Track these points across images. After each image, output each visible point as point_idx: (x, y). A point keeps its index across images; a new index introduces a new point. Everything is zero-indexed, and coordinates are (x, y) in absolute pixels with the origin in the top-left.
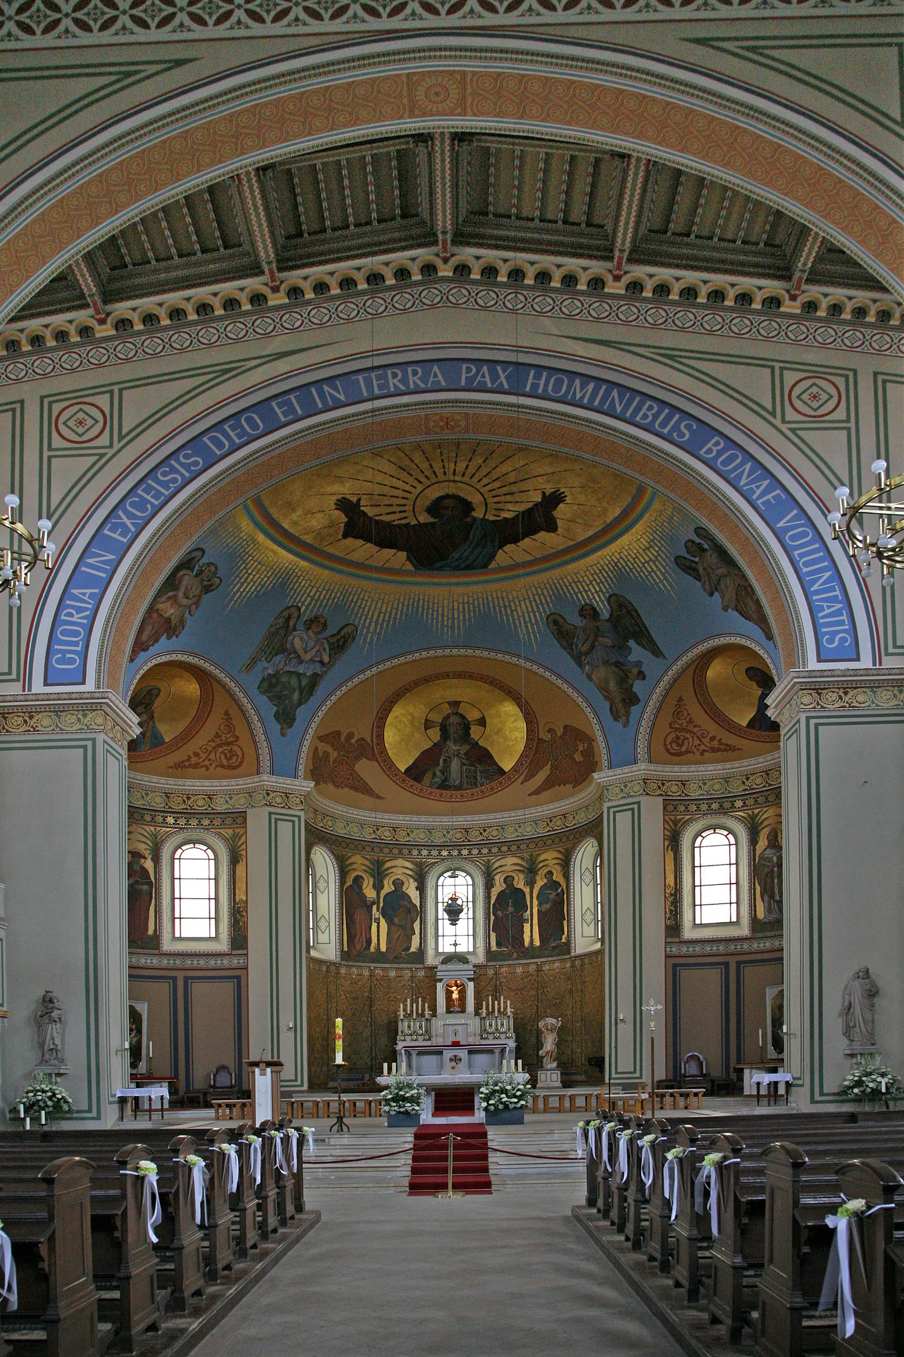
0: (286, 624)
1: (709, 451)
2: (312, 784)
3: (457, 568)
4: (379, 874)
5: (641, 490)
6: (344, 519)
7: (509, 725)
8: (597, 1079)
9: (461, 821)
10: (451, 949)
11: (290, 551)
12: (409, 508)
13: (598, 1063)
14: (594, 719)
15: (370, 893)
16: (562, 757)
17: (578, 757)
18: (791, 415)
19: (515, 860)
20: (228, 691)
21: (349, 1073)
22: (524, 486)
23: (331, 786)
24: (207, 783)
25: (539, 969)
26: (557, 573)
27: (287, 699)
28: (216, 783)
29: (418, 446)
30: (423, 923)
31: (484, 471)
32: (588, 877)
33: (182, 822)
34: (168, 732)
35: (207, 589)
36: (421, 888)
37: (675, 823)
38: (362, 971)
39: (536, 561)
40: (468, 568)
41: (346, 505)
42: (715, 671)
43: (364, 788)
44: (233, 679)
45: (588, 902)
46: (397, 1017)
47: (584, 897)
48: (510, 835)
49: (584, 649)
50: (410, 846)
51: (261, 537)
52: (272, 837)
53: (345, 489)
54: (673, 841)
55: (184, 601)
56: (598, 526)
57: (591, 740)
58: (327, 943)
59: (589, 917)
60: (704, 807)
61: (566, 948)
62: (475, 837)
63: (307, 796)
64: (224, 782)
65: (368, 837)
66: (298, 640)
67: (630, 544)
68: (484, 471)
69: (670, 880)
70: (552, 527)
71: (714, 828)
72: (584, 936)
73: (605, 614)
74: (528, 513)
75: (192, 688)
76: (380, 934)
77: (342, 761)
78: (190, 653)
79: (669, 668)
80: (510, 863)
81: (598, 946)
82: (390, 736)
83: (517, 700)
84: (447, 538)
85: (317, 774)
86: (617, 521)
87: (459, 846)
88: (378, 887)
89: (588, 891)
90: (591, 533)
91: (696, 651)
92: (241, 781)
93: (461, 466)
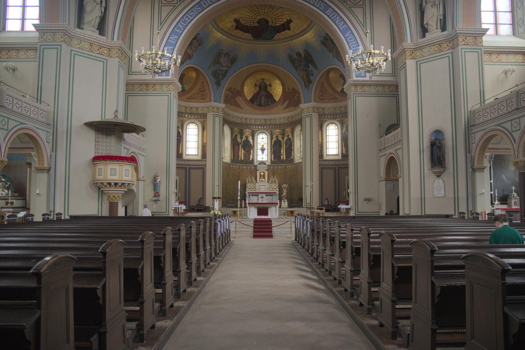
0: (219, 56)
1: (328, 12)
2: (225, 105)
3: (264, 39)
4: (242, 134)
5: (312, 21)
6: (236, 24)
7: (278, 87)
8: (300, 206)
9: (265, 117)
10: (261, 160)
11: (221, 33)
12: (252, 22)
13: (301, 200)
14: (300, 88)
15: (239, 140)
16: (292, 98)
17: (296, 98)
18: (349, 3)
19: (279, 131)
20: (203, 75)
21: (232, 199)
22: (283, 17)
23: (229, 105)
24: (197, 104)
25: (285, 168)
26: (290, 42)
27: (219, 77)
28: (199, 104)
29: (255, 5)
30: (253, 150)
31: (272, 12)
32: (298, 137)
33: (190, 116)
34: (187, 88)
35: (200, 45)
36: (253, 139)
37: (322, 121)
38: (237, 166)
39: (285, 39)
40: (267, 39)
41: (236, 21)
42: (332, 75)
43: (238, 106)
44: (205, 72)
45: (299, 146)
46: (246, 182)
47: (298, 144)
48: (278, 123)
49: (298, 65)
50: (250, 125)
51: (214, 30)
52: (214, 121)
53: (236, 16)
54: (321, 127)
55: (193, 49)
56: (301, 29)
57: (299, 94)
58: (227, 157)
59: (299, 150)
60: (329, 117)
61: (292, 161)
62: (268, 123)
63: (223, 109)
64: (201, 104)
65: (239, 122)
66: (222, 60)
67: (309, 36)
68: (272, 12)
69: (320, 140)
70: (289, 29)
71: (332, 123)
72: (297, 156)
73: (303, 54)
74: (283, 25)
75: (194, 75)
76: (242, 153)
77: (232, 98)
78: (194, 64)
79: (319, 73)
80: (277, 131)
81: (301, 160)
82: (246, 89)
83: (280, 79)
84: (262, 31)
85: (226, 102)
86: (306, 29)
87: (264, 125)
88: (241, 138)
89: (298, 141)
90: (299, 31)
91: (326, 69)
92: (206, 104)
93: (266, 11)
